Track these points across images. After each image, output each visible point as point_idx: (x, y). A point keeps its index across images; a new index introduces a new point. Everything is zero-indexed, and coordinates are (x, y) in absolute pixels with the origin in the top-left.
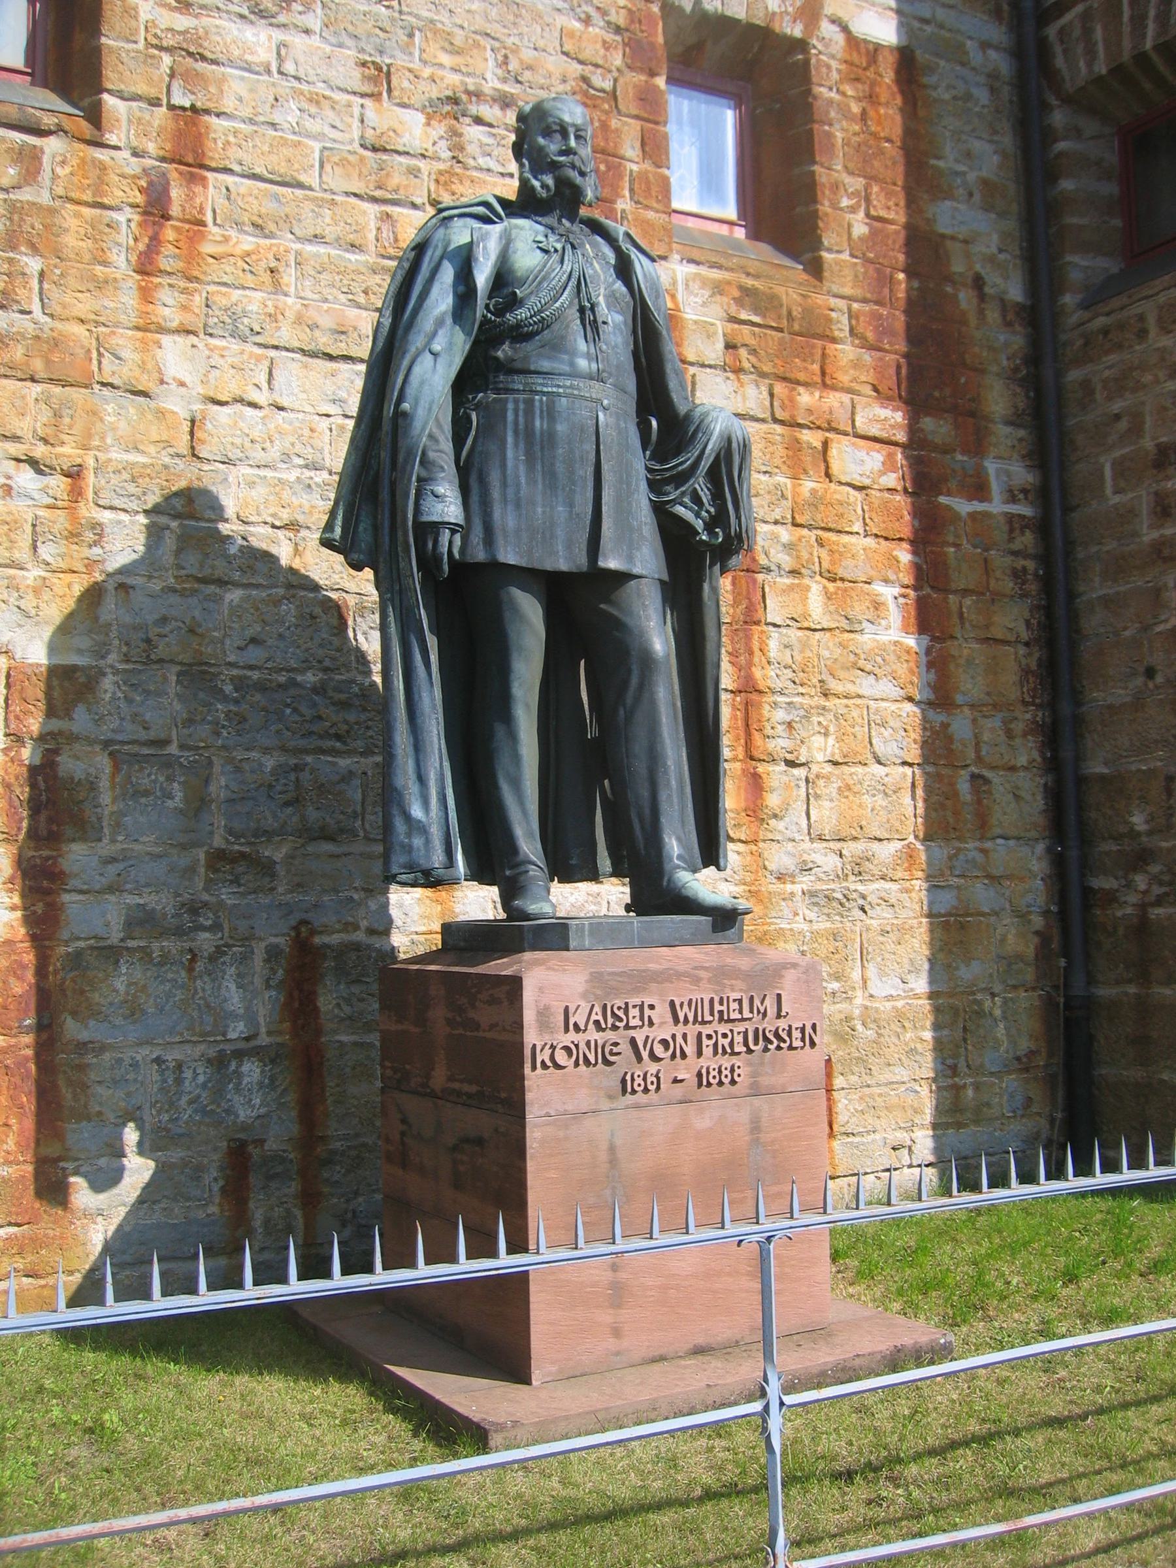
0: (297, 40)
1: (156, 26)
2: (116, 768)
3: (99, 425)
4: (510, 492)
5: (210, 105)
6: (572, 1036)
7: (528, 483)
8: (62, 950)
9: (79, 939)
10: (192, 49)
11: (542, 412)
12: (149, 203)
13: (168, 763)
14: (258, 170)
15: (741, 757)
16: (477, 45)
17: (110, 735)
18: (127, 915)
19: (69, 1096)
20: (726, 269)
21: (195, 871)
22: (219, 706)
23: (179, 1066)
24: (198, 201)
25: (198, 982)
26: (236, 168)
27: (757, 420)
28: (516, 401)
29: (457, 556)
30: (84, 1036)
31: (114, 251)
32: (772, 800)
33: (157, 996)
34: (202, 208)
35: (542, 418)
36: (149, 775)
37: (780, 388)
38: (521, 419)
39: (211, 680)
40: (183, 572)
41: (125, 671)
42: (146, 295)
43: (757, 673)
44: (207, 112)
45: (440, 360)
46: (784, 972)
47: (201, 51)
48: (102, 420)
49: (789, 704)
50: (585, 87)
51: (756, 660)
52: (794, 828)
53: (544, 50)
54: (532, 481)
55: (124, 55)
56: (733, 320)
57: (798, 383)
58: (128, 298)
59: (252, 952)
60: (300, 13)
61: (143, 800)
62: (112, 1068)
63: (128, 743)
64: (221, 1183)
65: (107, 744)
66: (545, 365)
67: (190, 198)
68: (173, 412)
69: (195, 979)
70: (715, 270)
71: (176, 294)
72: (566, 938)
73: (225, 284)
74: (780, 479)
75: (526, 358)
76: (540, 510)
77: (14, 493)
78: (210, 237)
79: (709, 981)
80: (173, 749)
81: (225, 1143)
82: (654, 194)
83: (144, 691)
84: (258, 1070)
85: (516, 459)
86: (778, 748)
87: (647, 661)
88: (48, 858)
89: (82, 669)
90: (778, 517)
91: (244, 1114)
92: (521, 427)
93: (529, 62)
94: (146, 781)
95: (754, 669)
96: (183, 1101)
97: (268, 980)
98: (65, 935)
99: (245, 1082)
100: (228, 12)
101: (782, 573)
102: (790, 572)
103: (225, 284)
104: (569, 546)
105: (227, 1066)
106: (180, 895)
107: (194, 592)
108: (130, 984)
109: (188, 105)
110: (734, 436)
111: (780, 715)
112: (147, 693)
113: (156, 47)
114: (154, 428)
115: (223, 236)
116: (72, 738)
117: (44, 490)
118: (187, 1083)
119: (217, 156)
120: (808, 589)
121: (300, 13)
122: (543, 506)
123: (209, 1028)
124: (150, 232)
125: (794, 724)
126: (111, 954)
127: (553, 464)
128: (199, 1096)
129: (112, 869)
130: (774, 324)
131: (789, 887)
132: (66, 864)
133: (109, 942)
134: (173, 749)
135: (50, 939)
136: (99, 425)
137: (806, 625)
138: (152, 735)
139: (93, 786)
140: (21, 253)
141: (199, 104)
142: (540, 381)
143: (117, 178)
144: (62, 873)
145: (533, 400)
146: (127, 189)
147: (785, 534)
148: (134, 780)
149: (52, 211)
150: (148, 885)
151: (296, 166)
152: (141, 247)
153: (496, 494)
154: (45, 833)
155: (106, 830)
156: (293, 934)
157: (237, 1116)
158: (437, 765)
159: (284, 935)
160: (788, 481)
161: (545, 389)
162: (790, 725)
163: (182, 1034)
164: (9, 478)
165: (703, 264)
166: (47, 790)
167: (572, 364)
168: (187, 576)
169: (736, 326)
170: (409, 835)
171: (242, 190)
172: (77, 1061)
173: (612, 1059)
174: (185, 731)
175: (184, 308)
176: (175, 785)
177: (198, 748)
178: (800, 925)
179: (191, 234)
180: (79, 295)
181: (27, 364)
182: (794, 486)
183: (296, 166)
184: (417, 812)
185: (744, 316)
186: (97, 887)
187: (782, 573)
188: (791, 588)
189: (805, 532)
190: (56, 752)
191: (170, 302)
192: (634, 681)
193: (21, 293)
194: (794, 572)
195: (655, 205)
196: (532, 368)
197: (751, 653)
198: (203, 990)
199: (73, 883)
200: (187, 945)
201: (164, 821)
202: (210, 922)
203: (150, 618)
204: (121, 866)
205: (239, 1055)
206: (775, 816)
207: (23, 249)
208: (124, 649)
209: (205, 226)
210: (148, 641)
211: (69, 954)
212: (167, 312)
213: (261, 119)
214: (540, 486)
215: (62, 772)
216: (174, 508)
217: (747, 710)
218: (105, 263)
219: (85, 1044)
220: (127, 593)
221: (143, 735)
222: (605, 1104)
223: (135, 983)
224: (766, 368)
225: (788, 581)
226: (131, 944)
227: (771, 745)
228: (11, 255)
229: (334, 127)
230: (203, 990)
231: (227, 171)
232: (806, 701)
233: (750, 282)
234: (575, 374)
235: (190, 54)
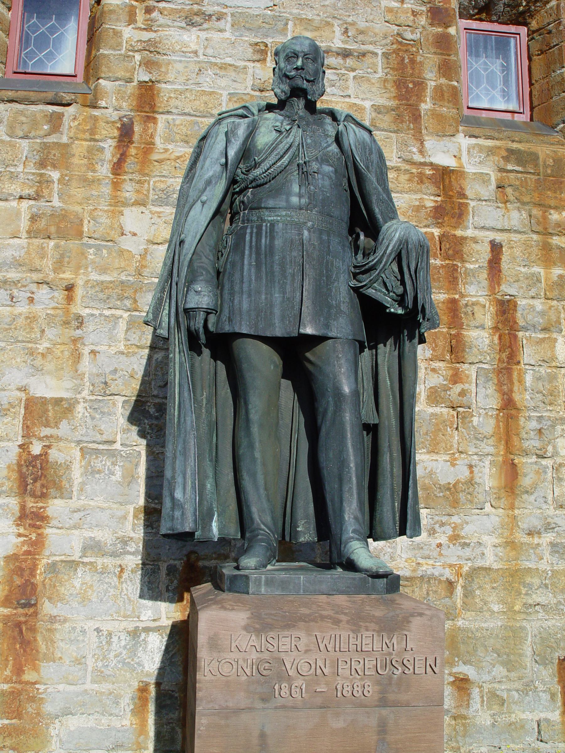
1: (132, 41)
2: (83, 456)
3: (84, 261)
4: (245, 286)
5: (159, 78)
6: (235, 655)
7: (255, 280)
8: (44, 561)
9: (55, 555)
10: (152, 49)
11: (266, 232)
12: (121, 135)
13: (112, 454)
14: (186, 111)
15: (502, 453)
16: (328, 24)
17: (80, 438)
18: (84, 543)
19: (44, 647)
20: (497, 139)
21: (126, 519)
22: (146, 421)
23: (110, 634)
24: (150, 131)
25: (124, 585)
26: (173, 110)
27: (520, 232)
28: (252, 228)
29: (211, 327)
30: (54, 612)
31: (100, 164)
32: (526, 481)
33: (99, 592)
34: (152, 135)
35: (266, 237)
36: (101, 461)
37: (535, 212)
38: (254, 239)
39: (142, 406)
40: (129, 343)
41: (91, 400)
42: (116, 186)
43: (516, 397)
45: (205, 206)
46: (411, 619)
47: (157, 50)
48: (86, 258)
49: (539, 417)
50: (400, 39)
51: (516, 388)
52: (542, 500)
53: (372, 22)
54: (258, 278)
55: (112, 58)
56: (501, 170)
57: (550, 207)
58: (107, 190)
59: (159, 569)
61: (97, 476)
62: (70, 632)
63: (91, 442)
64: (132, 707)
65: (79, 442)
66: (271, 203)
67: (145, 130)
68: (128, 251)
69: (122, 583)
70: (489, 140)
71: (134, 184)
72: (247, 586)
73: (164, 176)
74: (536, 269)
75: (260, 200)
76: (263, 297)
77: (34, 301)
78: (157, 151)
79: (348, 622)
80: (117, 446)
81: (137, 684)
82: (446, 98)
83: (101, 412)
84: (158, 641)
85: (250, 264)
86: (531, 447)
87: (338, 394)
88: (41, 508)
89: (67, 400)
90: (533, 295)
92: (254, 244)
93: (362, 29)
95: (514, 395)
97: (167, 587)
98: (47, 552)
99: (149, 647)
100: (174, 27)
101: (537, 330)
102: (542, 330)
103: (164, 176)
104: (283, 318)
105: (139, 637)
106: (116, 533)
107: (134, 354)
108: (82, 584)
109: (147, 80)
110: (410, 240)
111: (534, 424)
112: (103, 413)
113: (132, 51)
114: (117, 260)
115: (164, 149)
116: (59, 439)
117: (52, 298)
118: (114, 645)
119: (163, 105)
120: (556, 340)
122: (266, 294)
123: (129, 613)
124: (121, 152)
125: (543, 431)
126: (73, 565)
127: (272, 267)
129: (77, 516)
130: (532, 171)
131: (536, 540)
132: (50, 512)
133: (73, 558)
134: (117, 446)
135: (39, 555)
136: (84, 261)
137: (554, 364)
138: (105, 438)
139: (68, 468)
140: (48, 170)
141: (154, 79)
142: (267, 213)
143: (104, 124)
144: (48, 516)
145: (261, 226)
146: (109, 129)
147: (539, 305)
148: (92, 463)
149: (66, 146)
150: (97, 526)
151: (210, 106)
152: (115, 160)
153: (237, 288)
154: (39, 493)
155: (75, 493)
156: (185, 559)
158: (192, 464)
159: (180, 559)
160: (542, 271)
161: (269, 219)
162: (540, 431)
163: (112, 615)
164: (33, 293)
165: (480, 137)
166: (42, 468)
167: (288, 201)
169: (505, 174)
170: (173, 509)
171: (177, 122)
172: (49, 627)
173: (265, 673)
174: (125, 436)
175: (138, 191)
176: (117, 467)
178: (543, 566)
179: (145, 149)
180: (78, 189)
181: (47, 229)
182: (546, 274)
183: (210, 106)
184: (178, 495)
185: (510, 167)
186: (67, 526)
187: (537, 330)
188: (543, 340)
189: (555, 303)
190: (49, 447)
191: (130, 189)
192: (331, 409)
193: (46, 192)
194: (545, 329)
195: (446, 104)
196: (263, 206)
197: (512, 383)
198: (127, 589)
199: (53, 523)
200: (119, 563)
201: (109, 488)
202: (133, 550)
203: (107, 370)
204: (82, 514)
205: (147, 630)
206: (527, 492)
207: (49, 168)
208: (91, 388)
209: (154, 145)
210: (106, 383)
211: (48, 564)
212: (128, 194)
213: (191, 82)
214: (264, 281)
215: (51, 459)
216: (126, 306)
217: (508, 421)
218: (94, 171)
219: (55, 617)
220: (95, 355)
221: (99, 438)
222: (259, 705)
223: (86, 583)
224: (526, 199)
225: (541, 336)
226: (86, 560)
227: (526, 444)
228: (43, 171)
229: (235, 81)
230: (127, 589)
231: (168, 112)
232: (553, 415)
233: (515, 146)
234: (289, 207)
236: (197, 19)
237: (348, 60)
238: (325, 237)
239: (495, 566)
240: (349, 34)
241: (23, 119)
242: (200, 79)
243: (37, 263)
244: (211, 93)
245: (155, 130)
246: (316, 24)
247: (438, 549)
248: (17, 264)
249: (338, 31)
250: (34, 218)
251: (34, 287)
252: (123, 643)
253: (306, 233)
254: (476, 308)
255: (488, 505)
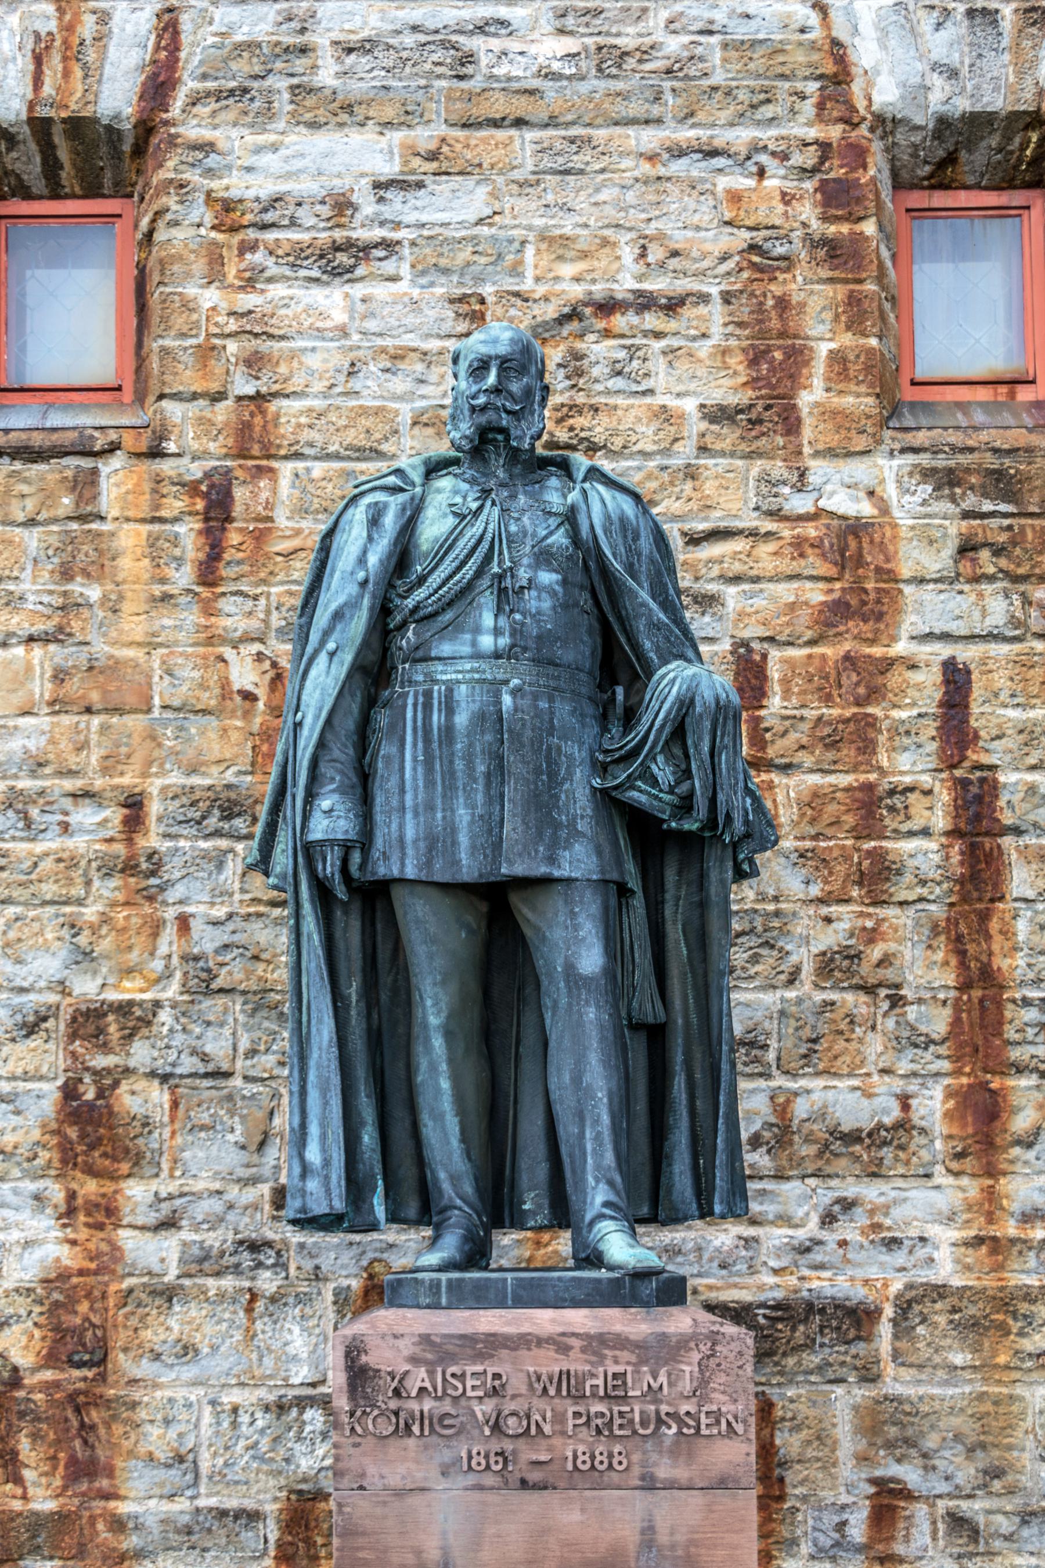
0: (381, 291)
10: (258, 329)
14: (332, 449)
16: (605, 242)
17: (168, 1069)
23: (235, 1410)
26: (307, 451)
44: (275, 395)
48: (160, 745)
60: (380, 259)
91: (306, 1464)
94: (206, 1115)
96: (239, 1448)
112: (208, 1024)
118: (244, 1428)
121: (380, 259)
128: (257, 1443)
141: (264, 390)
157: (298, 1466)
164: (67, 814)
168: (253, 900)
174: (249, 1062)
176: (237, 1119)
177: (263, 1080)
200: (247, 1284)
205: (302, 1403)
212: (228, 622)
218: (163, 581)
231: (298, 456)
235: (256, 335)
236: (342, 258)
237: (647, 316)
238: (543, 705)
239: (957, 1282)
240: (651, 259)
241: (25, 489)
242: (356, 384)
243: (73, 761)
244: (378, 411)
245: (274, 491)
246: (582, 245)
247: (841, 1251)
248: (38, 765)
249: (628, 254)
250: (59, 676)
251: (67, 803)
252: (260, 1424)
253: (507, 700)
254: (912, 797)
255: (939, 1169)
